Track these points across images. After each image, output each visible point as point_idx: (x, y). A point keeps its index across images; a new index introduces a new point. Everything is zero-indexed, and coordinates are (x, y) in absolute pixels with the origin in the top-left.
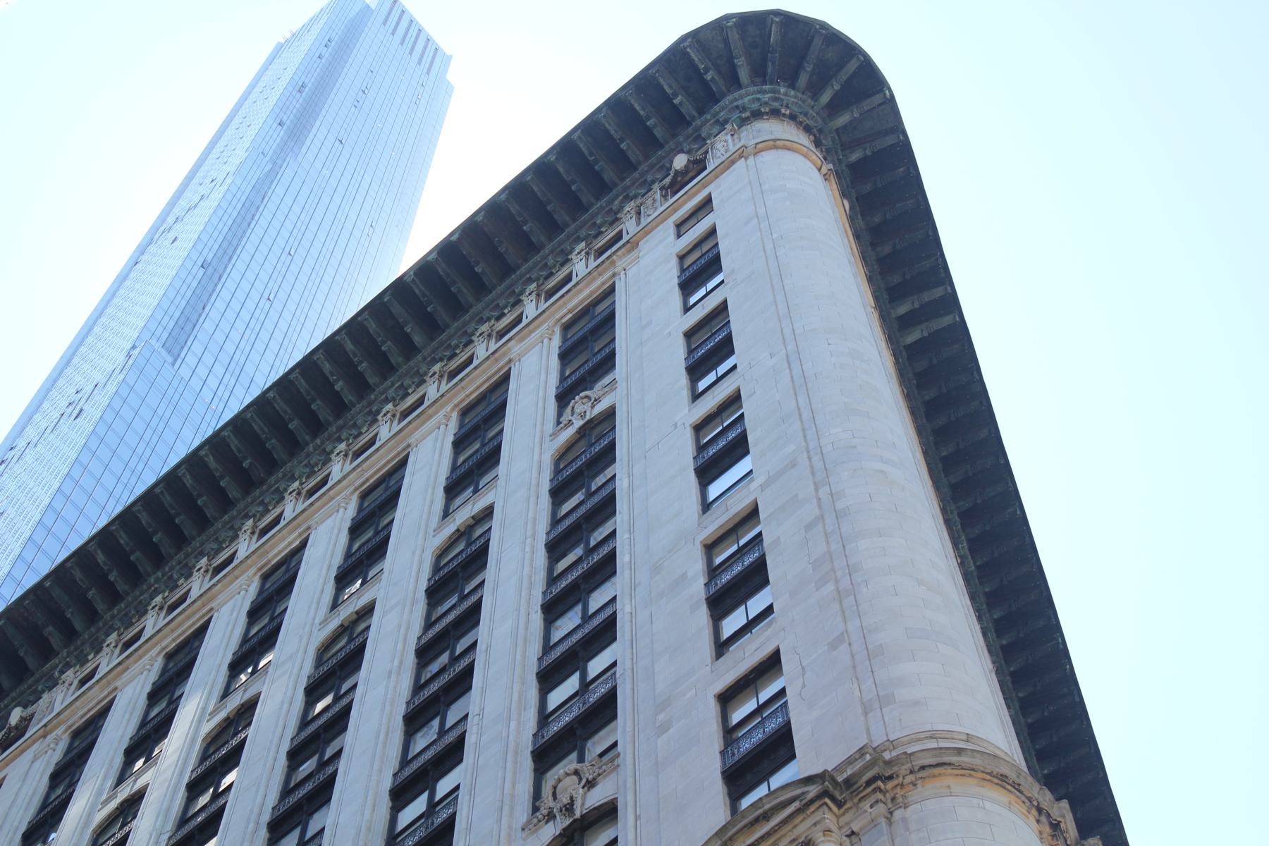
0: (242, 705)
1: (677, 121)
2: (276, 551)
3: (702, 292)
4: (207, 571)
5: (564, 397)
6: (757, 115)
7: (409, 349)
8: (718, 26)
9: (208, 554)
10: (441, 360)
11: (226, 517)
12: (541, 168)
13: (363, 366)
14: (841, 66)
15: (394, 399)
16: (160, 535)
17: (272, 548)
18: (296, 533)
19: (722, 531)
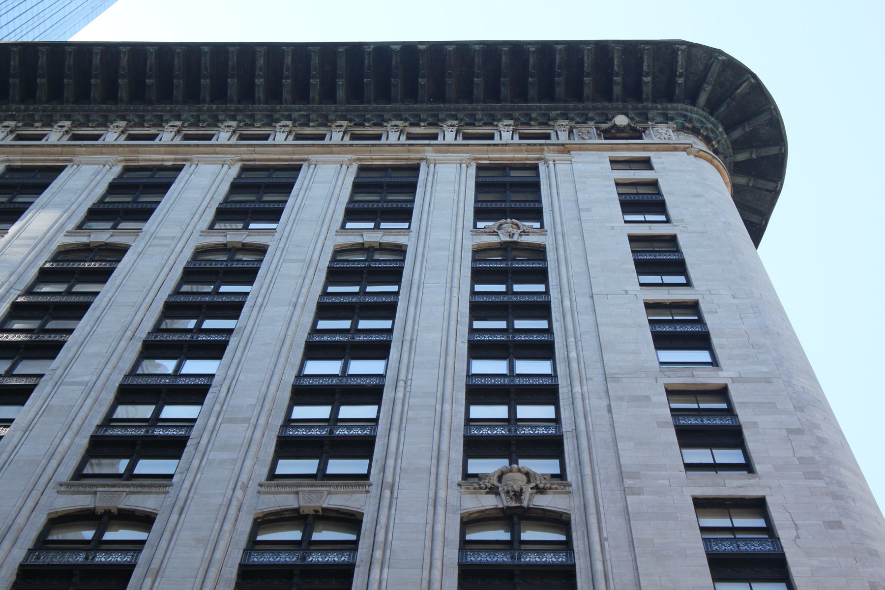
0: (106, 244)
1: (634, 92)
2: (148, 157)
3: (640, 218)
4: (67, 132)
5: (96, 214)
6: (695, 132)
7: (329, 95)
8: (712, 53)
9: (74, 122)
10: (350, 121)
11: (104, 107)
12: (517, 48)
13: (287, 82)
14: (765, 144)
15: (295, 121)
16: (44, 80)
17: (150, 153)
18: (173, 157)
19: (684, 388)
